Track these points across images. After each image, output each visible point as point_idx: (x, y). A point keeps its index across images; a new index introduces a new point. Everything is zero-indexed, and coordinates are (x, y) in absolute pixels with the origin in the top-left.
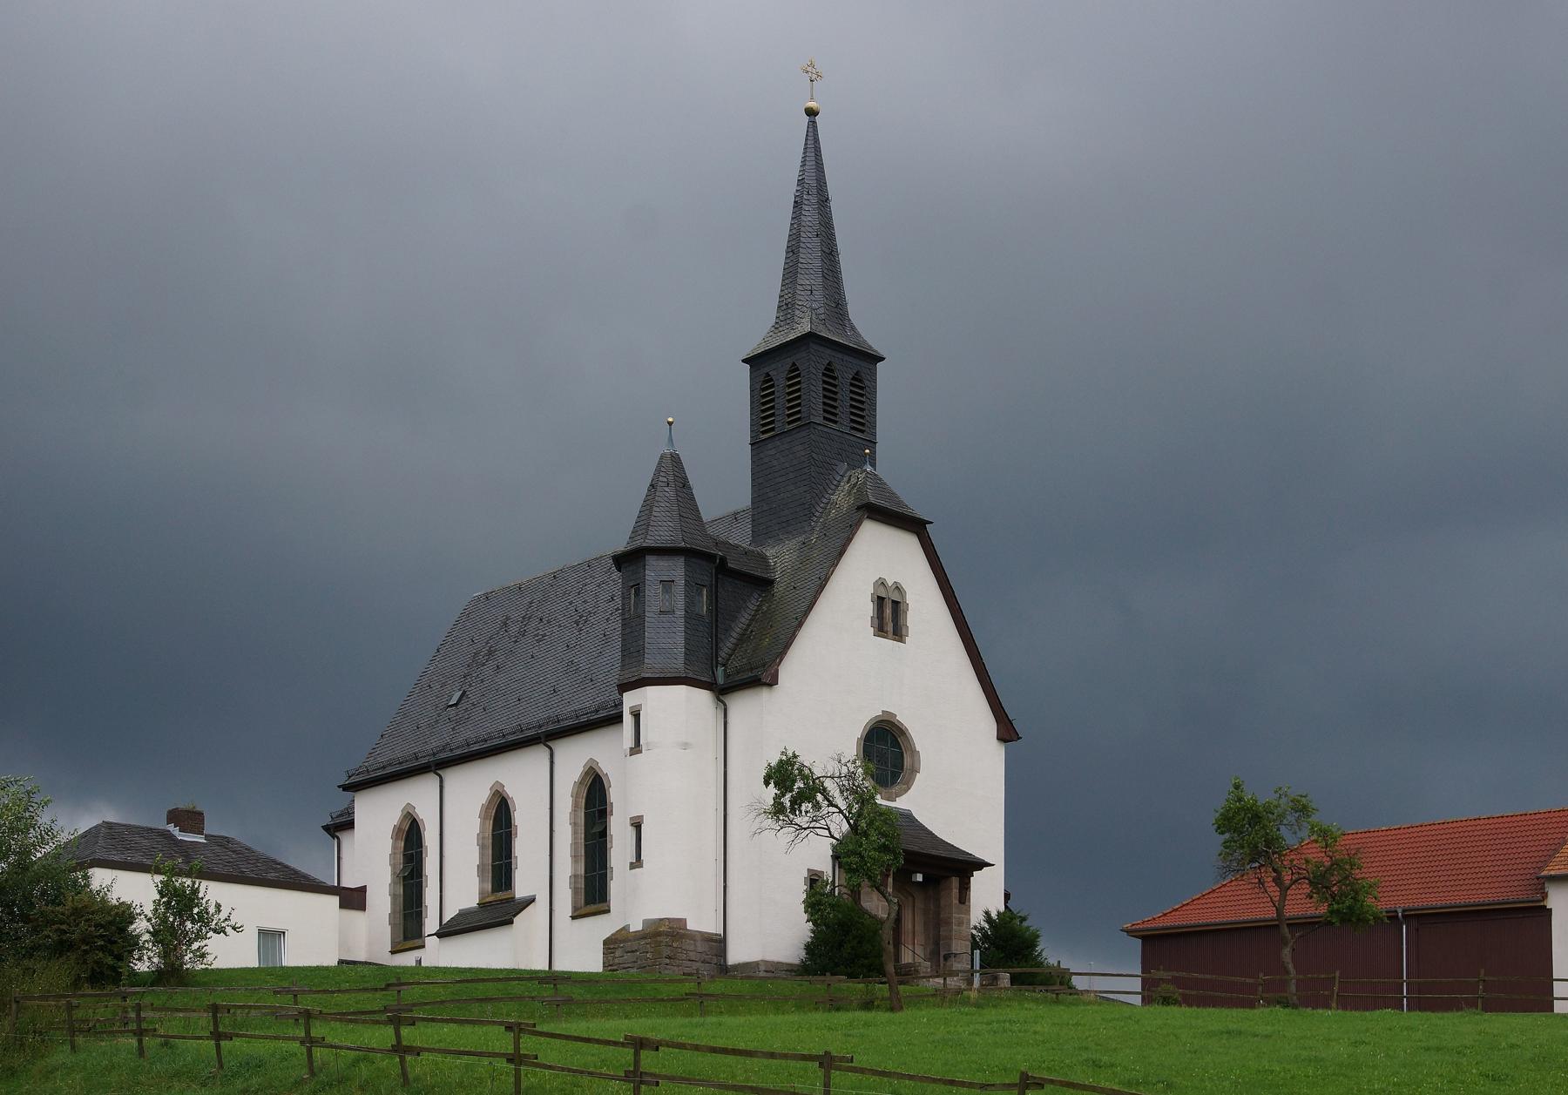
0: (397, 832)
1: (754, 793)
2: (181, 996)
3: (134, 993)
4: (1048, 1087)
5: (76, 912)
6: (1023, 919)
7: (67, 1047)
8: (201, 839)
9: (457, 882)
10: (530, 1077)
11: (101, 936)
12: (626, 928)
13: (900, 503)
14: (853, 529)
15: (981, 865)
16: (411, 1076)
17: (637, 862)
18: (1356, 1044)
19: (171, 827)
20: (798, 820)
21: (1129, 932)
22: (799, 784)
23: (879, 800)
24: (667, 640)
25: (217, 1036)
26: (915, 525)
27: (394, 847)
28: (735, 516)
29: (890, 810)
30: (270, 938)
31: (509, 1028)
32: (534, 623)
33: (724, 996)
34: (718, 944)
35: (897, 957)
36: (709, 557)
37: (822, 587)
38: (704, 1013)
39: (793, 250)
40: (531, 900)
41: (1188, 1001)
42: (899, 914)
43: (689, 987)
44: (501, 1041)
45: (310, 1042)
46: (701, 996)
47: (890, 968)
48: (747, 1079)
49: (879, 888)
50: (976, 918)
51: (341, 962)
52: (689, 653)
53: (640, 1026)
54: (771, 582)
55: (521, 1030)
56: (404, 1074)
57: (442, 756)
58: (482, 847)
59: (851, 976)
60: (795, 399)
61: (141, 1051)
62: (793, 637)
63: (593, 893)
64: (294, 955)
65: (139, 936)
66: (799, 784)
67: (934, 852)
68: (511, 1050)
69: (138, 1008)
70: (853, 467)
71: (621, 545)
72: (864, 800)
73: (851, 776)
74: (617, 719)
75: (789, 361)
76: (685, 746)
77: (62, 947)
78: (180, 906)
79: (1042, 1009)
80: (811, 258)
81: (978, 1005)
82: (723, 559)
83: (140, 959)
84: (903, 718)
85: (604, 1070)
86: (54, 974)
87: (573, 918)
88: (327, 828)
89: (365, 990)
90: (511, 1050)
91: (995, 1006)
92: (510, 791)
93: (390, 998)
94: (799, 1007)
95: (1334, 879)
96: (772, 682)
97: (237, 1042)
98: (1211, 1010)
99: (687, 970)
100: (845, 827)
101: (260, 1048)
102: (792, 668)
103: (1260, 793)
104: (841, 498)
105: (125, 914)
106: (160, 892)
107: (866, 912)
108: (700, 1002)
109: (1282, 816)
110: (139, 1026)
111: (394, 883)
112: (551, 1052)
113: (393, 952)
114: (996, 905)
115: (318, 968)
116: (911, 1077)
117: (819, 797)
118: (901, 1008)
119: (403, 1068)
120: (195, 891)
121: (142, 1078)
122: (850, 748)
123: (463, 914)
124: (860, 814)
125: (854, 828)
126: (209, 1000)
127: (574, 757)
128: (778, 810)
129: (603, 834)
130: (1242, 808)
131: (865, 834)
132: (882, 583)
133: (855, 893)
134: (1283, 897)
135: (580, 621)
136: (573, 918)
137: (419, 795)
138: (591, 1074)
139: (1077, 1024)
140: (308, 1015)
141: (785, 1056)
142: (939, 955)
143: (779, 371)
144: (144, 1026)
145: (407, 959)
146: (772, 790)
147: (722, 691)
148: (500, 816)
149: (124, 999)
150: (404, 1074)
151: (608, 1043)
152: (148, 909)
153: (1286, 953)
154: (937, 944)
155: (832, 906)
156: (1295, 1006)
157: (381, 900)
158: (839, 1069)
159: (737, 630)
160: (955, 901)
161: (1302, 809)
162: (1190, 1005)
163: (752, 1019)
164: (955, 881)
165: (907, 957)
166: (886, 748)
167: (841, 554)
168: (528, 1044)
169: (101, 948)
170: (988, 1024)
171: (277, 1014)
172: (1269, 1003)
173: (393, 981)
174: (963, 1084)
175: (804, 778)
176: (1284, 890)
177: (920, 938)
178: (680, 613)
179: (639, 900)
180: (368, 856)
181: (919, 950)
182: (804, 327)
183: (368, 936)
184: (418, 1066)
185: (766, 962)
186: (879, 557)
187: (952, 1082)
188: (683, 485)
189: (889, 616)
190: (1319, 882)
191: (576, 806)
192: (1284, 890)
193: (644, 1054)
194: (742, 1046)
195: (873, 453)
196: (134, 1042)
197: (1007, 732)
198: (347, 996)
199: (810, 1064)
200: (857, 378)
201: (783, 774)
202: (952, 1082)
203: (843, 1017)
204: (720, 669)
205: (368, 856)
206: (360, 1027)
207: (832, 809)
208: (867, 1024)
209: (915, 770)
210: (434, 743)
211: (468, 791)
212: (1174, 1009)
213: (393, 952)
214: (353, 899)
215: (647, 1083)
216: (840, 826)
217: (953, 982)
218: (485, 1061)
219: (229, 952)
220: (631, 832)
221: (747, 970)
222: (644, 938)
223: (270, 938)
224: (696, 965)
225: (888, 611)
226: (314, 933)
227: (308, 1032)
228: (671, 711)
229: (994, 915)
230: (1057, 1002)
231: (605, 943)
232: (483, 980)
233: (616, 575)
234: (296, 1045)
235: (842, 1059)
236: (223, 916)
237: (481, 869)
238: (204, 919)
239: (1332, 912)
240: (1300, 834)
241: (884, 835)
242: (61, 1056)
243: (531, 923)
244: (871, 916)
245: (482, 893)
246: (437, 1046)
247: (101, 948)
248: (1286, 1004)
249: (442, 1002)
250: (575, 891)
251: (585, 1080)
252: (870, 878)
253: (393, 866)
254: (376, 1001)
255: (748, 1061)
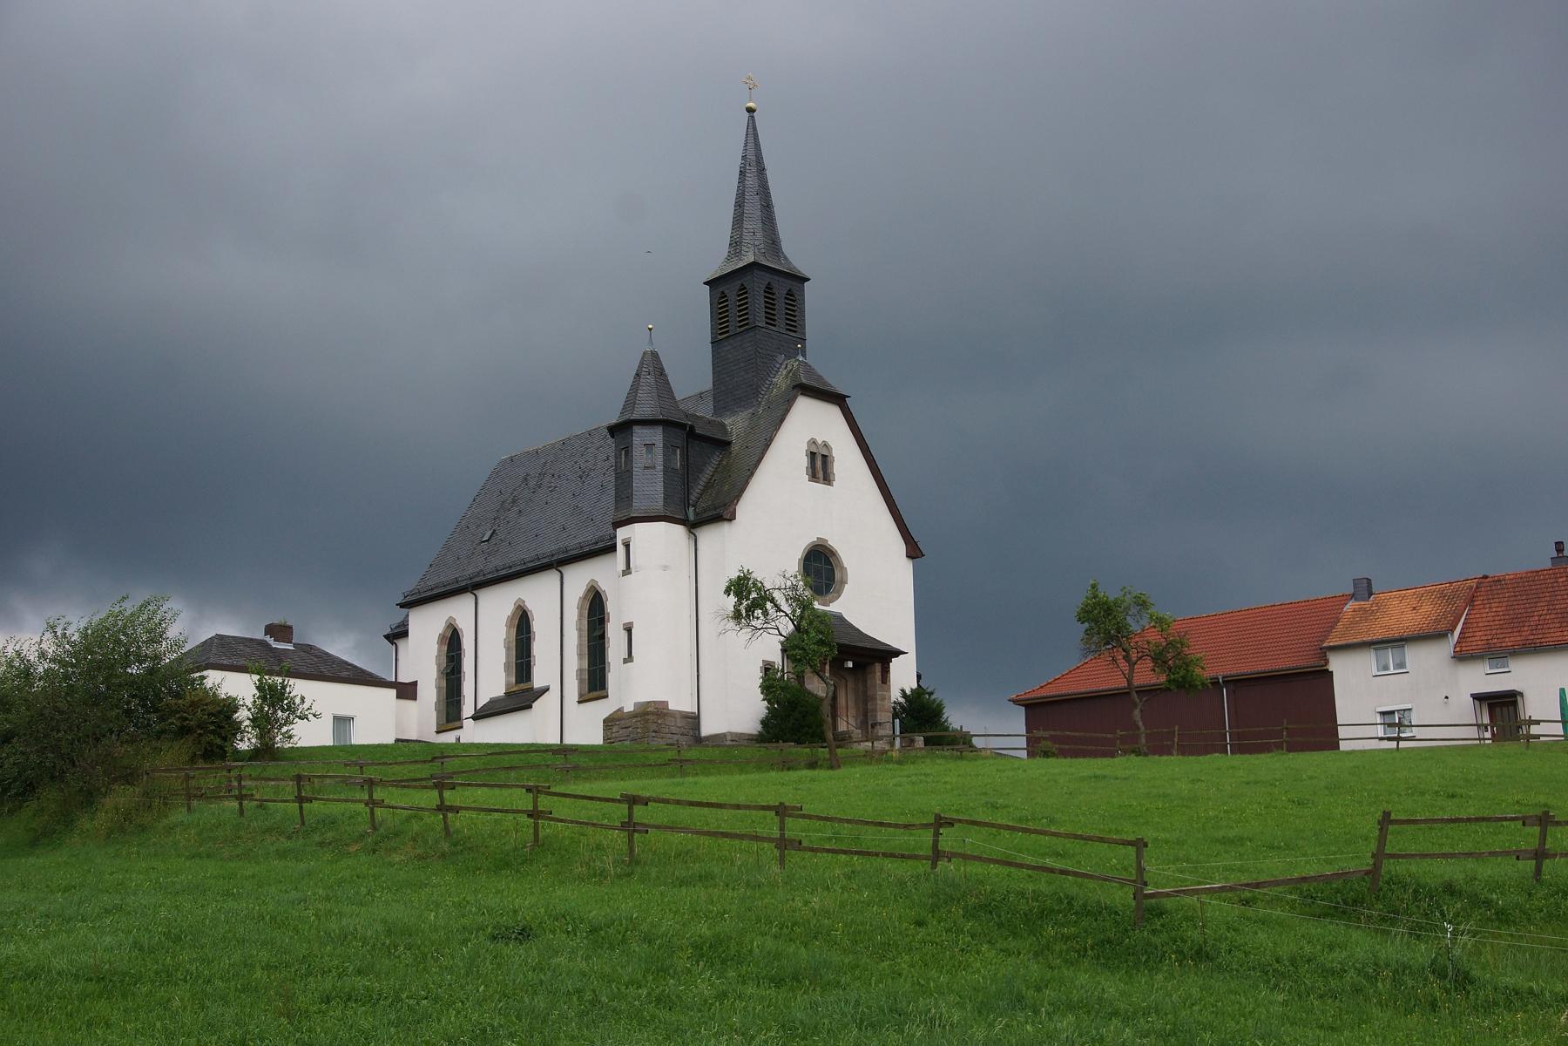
0: (442, 638)
2: (272, 769)
4: (957, 825)
5: (193, 704)
7: (184, 810)
9: (488, 676)
10: (547, 829)
12: (620, 710)
13: (825, 383)
15: (898, 653)
17: (629, 658)
19: (268, 638)
22: (754, 595)
23: (816, 605)
24: (650, 486)
25: (301, 800)
28: (701, 395)
29: (825, 613)
30: (342, 722)
31: (529, 790)
32: (547, 478)
33: (699, 761)
34: (694, 720)
36: (681, 426)
37: (768, 446)
39: (740, 204)
40: (547, 689)
41: (1063, 754)
43: (672, 754)
44: (523, 800)
45: (372, 803)
47: (830, 735)
48: (719, 826)
49: (819, 673)
50: (895, 695)
51: (397, 740)
53: (633, 786)
54: (729, 443)
56: (446, 828)
59: (799, 742)
60: (744, 309)
62: (746, 483)
63: (595, 683)
64: (361, 736)
66: (754, 595)
69: (240, 778)
71: (614, 421)
72: (805, 606)
73: (794, 588)
74: (612, 549)
76: (665, 568)
77: (184, 731)
78: (272, 697)
79: (951, 765)
80: (753, 208)
81: (899, 763)
82: (692, 427)
84: (834, 543)
86: (173, 753)
88: (387, 637)
92: (530, 606)
94: (759, 768)
96: (732, 518)
97: (315, 804)
100: (791, 627)
101: (335, 809)
102: (747, 507)
103: (1110, 593)
104: (781, 380)
105: (231, 706)
107: (809, 693)
108: (680, 766)
109: (1127, 609)
111: (439, 678)
112: (563, 809)
114: (910, 683)
115: (379, 745)
116: (848, 821)
117: (769, 605)
120: (284, 687)
121: (242, 833)
122: (793, 565)
123: (493, 701)
124: (802, 617)
125: (797, 628)
126: (295, 771)
127: (579, 578)
128: (737, 616)
129: (603, 636)
132: (813, 442)
133: (800, 677)
134: (1132, 670)
137: (459, 610)
140: (371, 783)
141: (748, 807)
142: (868, 724)
143: (731, 291)
145: (449, 738)
146: (733, 599)
148: (522, 625)
150: (446, 828)
151: (607, 800)
153: (1137, 712)
154: (865, 715)
156: (1146, 755)
157: (429, 692)
158: (791, 816)
161: (1142, 604)
164: (878, 667)
165: (842, 727)
166: (821, 566)
167: (782, 421)
168: (544, 802)
169: (213, 732)
171: (346, 781)
172: (1125, 752)
174: (890, 825)
176: (1132, 665)
177: (852, 712)
178: (660, 468)
179: (631, 687)
181: (851, 721)
182: (749, 258)
183: (417, 720)
184: (458, 822)
186: (810, 422)
187: (881, 824)
188: (661, 373)
189: (820, 466)
190: (1159, 659)
191: (580, 615)
192: (1132, 665)
194: (714, 800)
195: (804, 346)
196: (235, 804)
197: (914, 552)
200: (790, 293)
202: (881, 824)
205: (420, 658)
206: (412, 791)
208: (813, 780)
209: (843, 582)
210: (471, 570)
211: (497, 605)
212: (1052, 761)
214: (407, 691)
216: (787, 627)
217: (879, 745)
218: (510, 817)
219: (310, 734)
220: (625, 635)
221: (717, 740)
223: (342, 722)
225: (819, 463)
226: (377, 719)
227: (371, 795)
228: (654, 543)
230: (961, 758)
233: (610, 441)
235: (794, 808)
236: (306, 706)
237: (507, 666)
238: (291, 709)
242: (179, 815)
243: (546, 707)
245: (507, 685)
247: (213, 732)
248: (1138, 753)
250: (581, 682)
251: (590, 830)
253: (439, 665)
254: (424, 771)
255: (719, 811)
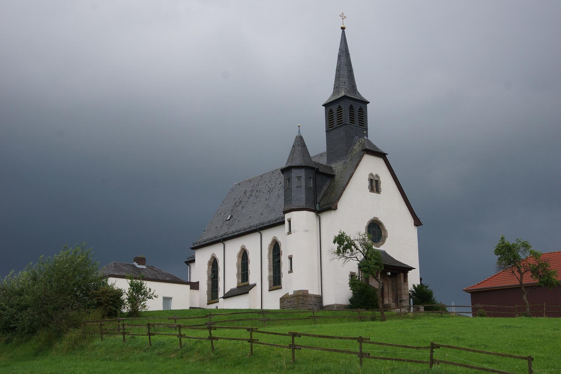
0: (210, 263)
1: (330, 246)
2: (137, 321)
3: (122, 320)
4: (441, 348)
5: (103, 293)
6: (427, 287)
7: (100, 339)
8: (144, 267)
9: (230, 279)
10: (256, 347)
11: (111, 301)
12: (287, 294)
13: (377, 148)
14: (361, 157)
15: (411, 269)
16: (215, 347)
17: (291, 271)
18: (554, 330)
19: (135, 263)
20: (346, 255)
21: (465, 291)
22: (346, 243)
23: (374, 247)
24: (300, 196)
25: (150, 334)
26: (382, 155)
27: (208, 268)
28: (321, 155)
29: (378, 251)
30: (167, 300)
31: (248, 330)
32: (255, 192)
33: (322, 317)
34: (320, 298)
35: (383, 302)
36: (313, 168)
37: (351, 177)
38: (315, 323)
39: (338, 70)
40: (255, 285)
41: (490, 315)
42: (383, 286)
43: (310, 314)
44: (246, 334)
45: (180, 336)
46: (314, 317)
47: (381, 306)
48: (332, 347)
49: (375, 278)
50: (410, 287)
51: (191, 308)
52: (307, 200)
53: (294, 328)
54: (333, 176)
55: (252, 331)
56: (213, 347)
57: (225, 237)
58: (238, 267)
59: (367, 309)
60: (340, 116)
61: (124, 339)
62: (342, 193)
63: (276, 282)
64: (175, 306)
65: (124, 300)
66: (346, 243)
67: (394, 265)
68: (249, 338)
69: (124, 325)
70: (361, 137)
71: (284, 165)
72: (369, 248)
73: (364, 239)
74: (283, 223)
75: (338, 105)
76: (306, 231)
77: (99, 304)
78: (137, 289)
79: (437, 320)
80: (345, 73)
81: (413, 318)
82: (318, 169)
83: (124, 308)
84: (381, 219)
85: (282, 344)
86: (96, 313)
87: (269, 291)
88: (186, 262)
89: (199, 317)
90: (249, 338)
91: (419, 319)
92: (247, 248)
93: (207, 320)
94: (349, 321)
95: (540, 270)
96: (336, 209)
97: (156, 336)
98: (499, 318)
99: (309, 308)
100: (363, 257)
101: (164, 339)
102: (342, 204)
103: (511, 241)
104: (357, 148)
105: (119, 293)
106: (130, 285)
107: (371, 286)
108: (314, 319)
109: (519, 248)
110: (124, 331)
111: (208, 280)
112: (263, 338)
113: (208, 304)
114: (417, 282)
115: (183, 310)
116: (391, 345)
117: (353, 247)
118: (385, 320)
119: (212, 344)
120: (142, 284)
121: (124, 349)
122: (363, 230)
123: (232, 290)
124: (367, 253)
125: (366, 257)
126: (146, 322)
127: (268, 236)
128: (338, 252)
129: (279, 261)
130: (505, 246)
131: (370, 259)
132: (372, 174)
133: (367, 280)
134: (522, 277)
135: (270, 191)
136: (269, 291)
137: (217, 250)
138: (277, 346)
139: (450, 324)
140: (180, 327)
141: (345, 338)
142: (398, 301)
143: (335, 108)
144: (125, 331)
145: (213, 306)
146: (337, 245)
147: (318, 212)
148: (244, 256)
149: (119, 322)
150: (213, 347)
151: (283, 334)
152: (127, 291)
153: (525, 297)
154: (397, 296)
155: (359, 284)
156: (530, 316)
157: (204, 286)
158: (365, 342)
159: (322, 192)
160: (403, 282)
161: (526, 246)
162: (490, 316)
163: (333, 325)
164: (402, 275)
165: (386, 302)
166: (376, 230)
167: (357, 166)
168: (255, 335)
169: (111, 305)
170: (417, 325)
171: (169, 326)
172: (520, 315)
173: (208, 314)
174: (410, 347)
175: (348, 241)
176: (522, 275)
177: (391, 295)
178: (304, 187)
179: (292, 284)
180: (199, 271)
181: (391, 299)
182: (343, 94)
183: (200, 298)
184: (218, 344)
185: (336, 305)
186: (370, 166)
187: (406, 347)
188: (304, 145)
189: (375, 185)
190: (535, 272)
191: (269, 252)
192: (522, 275)
193: (295, 338)
194: (330, 335)
195: (367, 132)
196: (122, 337)
197: (417, 223)
198: (193, 320)
199: (354, 341)
200: (361, 109)
201: (340, 239)
202: (406, 347)
203: (365, 324)
204: (318, 205)
205: (199, 271)
206: (197, 330)
207: (358, 251)
208: (373, 326)
209: (386, 237)
210: (222, 233)
211: (233, 249)
212: (485, 319)
213: (208, 304)
214: (195, 286)
215: (297, 349)
216: (361, 257)
217: (403, 310)
218: (240, 342)
219: (153, 305)
220: (288, 261)
221: (330, 307)
222: (294, 297)
223: (167, 300)
224: (312, 306)
225: (374, 184)
226: (182, 298)
227: (180, 333)
228: (301, 219)
229: (416, 286)
230: (441, 316)
231: (280, 299)
232: (239, 313)
233: (282, 175)
234: (176, 337)
235: (366, 339)
236: (151, 293)
237: (238, 275)
238: (145, 294)
239: (540, 282)
240: (526, 255)
241: (376, 259)
242: (97, 342)
243: (255, 293)
244: (373, 287)
245: (238, 283)
246: (224, 337)
247: (111, 305)
248: (526, 316)
249: (225, 321)
250: (270, 282)
251: (275, 347)
252: (372, 274)
253: (208, 274)
254: (202, 321)
255: (332, 340)
